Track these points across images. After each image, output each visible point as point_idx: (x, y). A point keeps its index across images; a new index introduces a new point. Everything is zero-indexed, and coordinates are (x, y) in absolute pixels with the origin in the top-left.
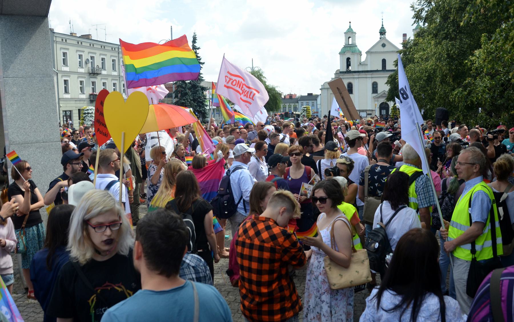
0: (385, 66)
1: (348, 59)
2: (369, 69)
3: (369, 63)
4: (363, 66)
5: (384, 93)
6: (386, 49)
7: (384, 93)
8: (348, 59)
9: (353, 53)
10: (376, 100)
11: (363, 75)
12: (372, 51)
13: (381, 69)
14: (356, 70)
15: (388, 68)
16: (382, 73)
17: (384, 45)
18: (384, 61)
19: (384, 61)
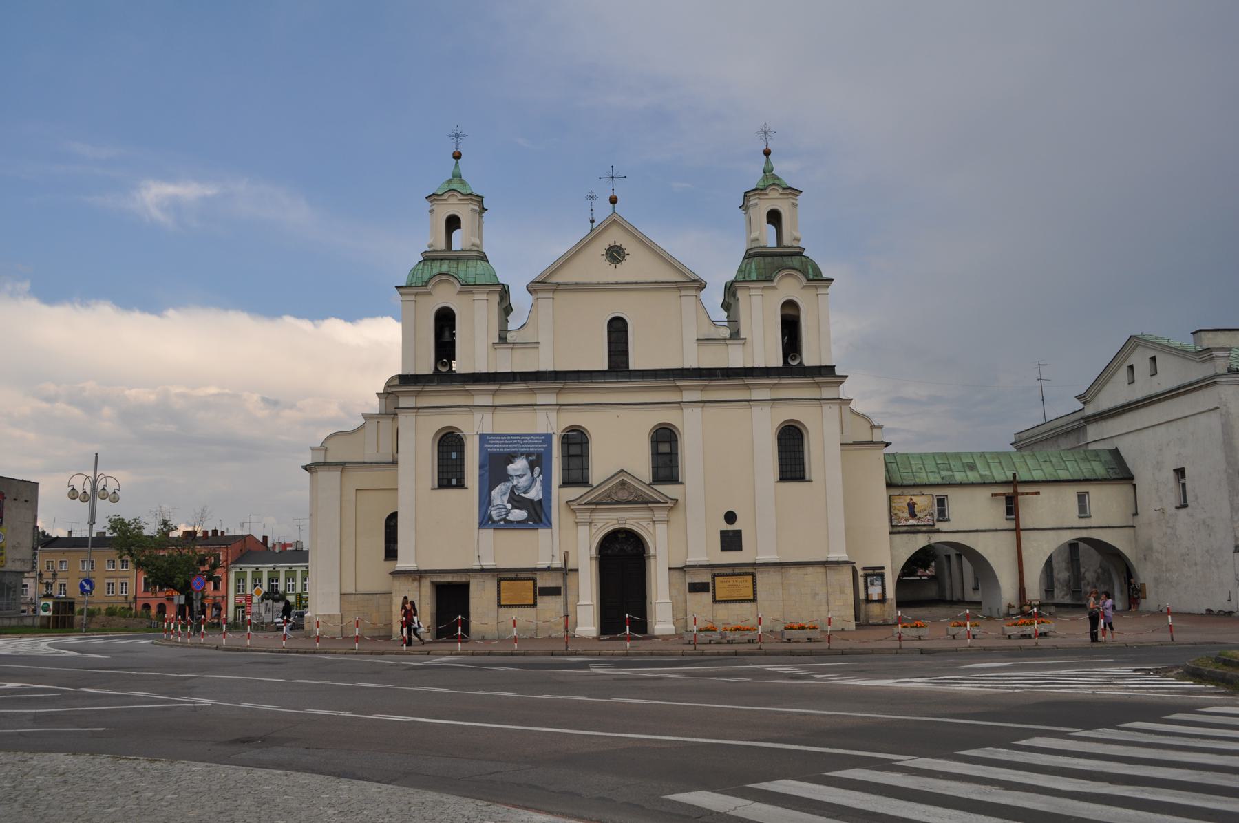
0: (625, 353)
1: (445, 320)
2: (546, 365)
3: (544, 338)
4: (518, 353)
5: (623, 483)
6: (624, 272)
7: (623, 483)
8: (445, 320)
9: (468, 287)
10: (586, 516)
12: (558, 278)
13: (604, 366)
14: (481, 367)
15: (637, 361)
16: (611, 383)
17: (615, 254)
18: (618, 330)
19: (618, 330)
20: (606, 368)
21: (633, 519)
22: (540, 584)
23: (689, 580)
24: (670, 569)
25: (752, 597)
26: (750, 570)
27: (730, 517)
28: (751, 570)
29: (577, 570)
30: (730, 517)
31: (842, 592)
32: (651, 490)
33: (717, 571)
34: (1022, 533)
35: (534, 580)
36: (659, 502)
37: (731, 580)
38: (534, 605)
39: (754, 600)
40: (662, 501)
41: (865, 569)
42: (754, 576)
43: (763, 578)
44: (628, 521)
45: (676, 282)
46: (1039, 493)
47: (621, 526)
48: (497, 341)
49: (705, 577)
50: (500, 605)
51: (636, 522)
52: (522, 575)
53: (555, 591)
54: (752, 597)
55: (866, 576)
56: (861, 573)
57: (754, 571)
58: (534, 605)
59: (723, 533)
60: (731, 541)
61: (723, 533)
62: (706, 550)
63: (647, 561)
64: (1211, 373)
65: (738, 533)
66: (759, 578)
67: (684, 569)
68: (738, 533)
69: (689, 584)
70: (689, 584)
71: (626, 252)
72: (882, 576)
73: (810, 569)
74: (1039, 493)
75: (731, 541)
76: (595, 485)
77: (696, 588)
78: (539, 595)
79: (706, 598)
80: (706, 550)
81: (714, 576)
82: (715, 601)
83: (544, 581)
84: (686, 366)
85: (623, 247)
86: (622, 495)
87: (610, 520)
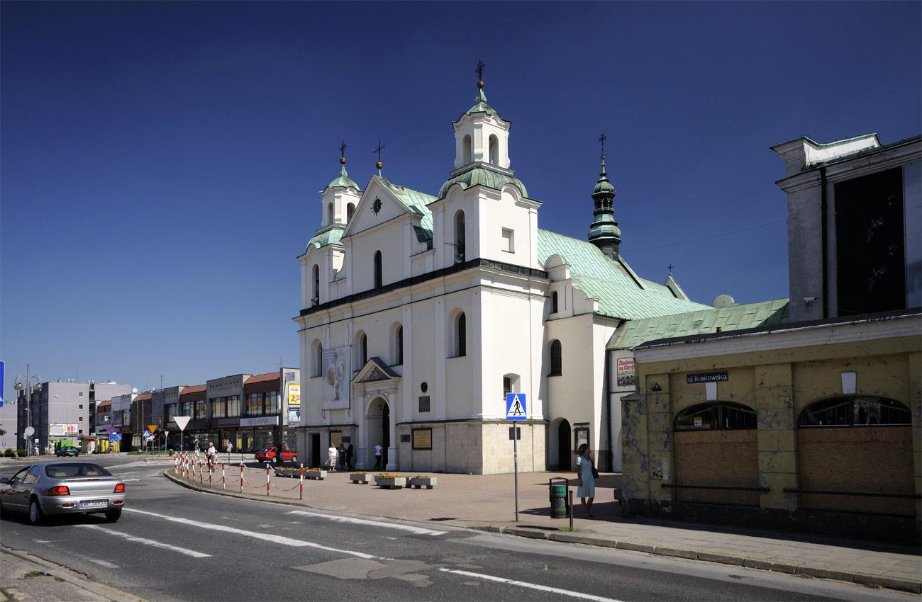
27: (424, 387)
30: (424, 387)
33: (415, 426)
37: (421, 432)
39: (431, 449)
41: (575, 424)
42: (431, 429)
55: (576, 431)
56: (573, 428)
60: (424, 404)
65: (428, 398)
68: (428, 398)
72: (588, 430)
75: (424, 404)
79: (408, 445)
81: (413, 430)
82: (414, 448)
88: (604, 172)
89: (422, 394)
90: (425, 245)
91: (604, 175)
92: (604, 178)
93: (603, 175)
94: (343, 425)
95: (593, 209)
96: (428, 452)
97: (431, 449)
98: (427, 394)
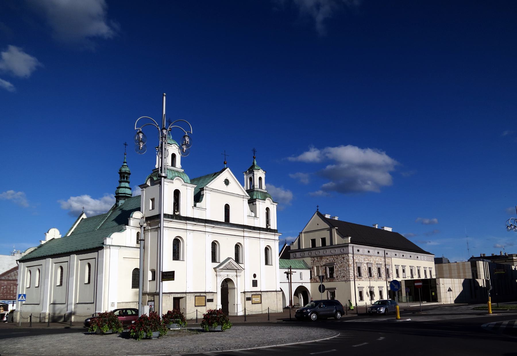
11: (200, 227)
15: (232, 221)
18: (227, 207)
19: (227, 207)
20: (224, 221)
21: (231, 275)
22: (207, 298)
23: (246, 297)
24: (241, 293)
25: (260, 302)
26: (260, 293)
27: (255, 276)
28: (259, 294)
29: (217, 293)
30: (255, 276)
31: (280, 300)
32: (238, 265)
33: (253, 293)
34: (292, 283)
35: (205, 296)
36: (239, 270)
38: (205, 306)
39: (261, 303)
40: (240, 269)
42: (261, 295)
43: (264, 295)
44: (230, 276)
45: (243, 196)
46: (296, 272)
47: (228, 277)
48: (193, 206)
49: (249, 295)
50: (195, 306)
51: (232, 276)
52: (202, 294)
53: (211, 300)
54: (260, 302)
57: (261, 293)
58: (205, 306)
59: (253, 280)
60: (255, 283)
61: (253, 280)
62: (249, 287)
63: (229, 291)
64: (344, 242)
66: (262, 295)
67: (244, 292)
69: (246, 298)
70: (246, 298)
71: (230, 182)
73: (273, 292)
74: (296, 272)
75: (255, 283)
76: (221, 261)
77: (248, 299)
78: (207, 302)
79: (250, 302)
80: (249, 287)
83: (209, 297)
84: (245, 224)
85: (229, 180)
86: (229, 267)
87: (225, 275)
88: (125, 161)
89: (254, 279)
90: (253, 214)
91: (126, 163)
92: (125, 164)
93: (124, 162)
94: (186, 293)
95: (119, 179)
96: (259, 305)
97: (261, 303)
98: (256, 279)
